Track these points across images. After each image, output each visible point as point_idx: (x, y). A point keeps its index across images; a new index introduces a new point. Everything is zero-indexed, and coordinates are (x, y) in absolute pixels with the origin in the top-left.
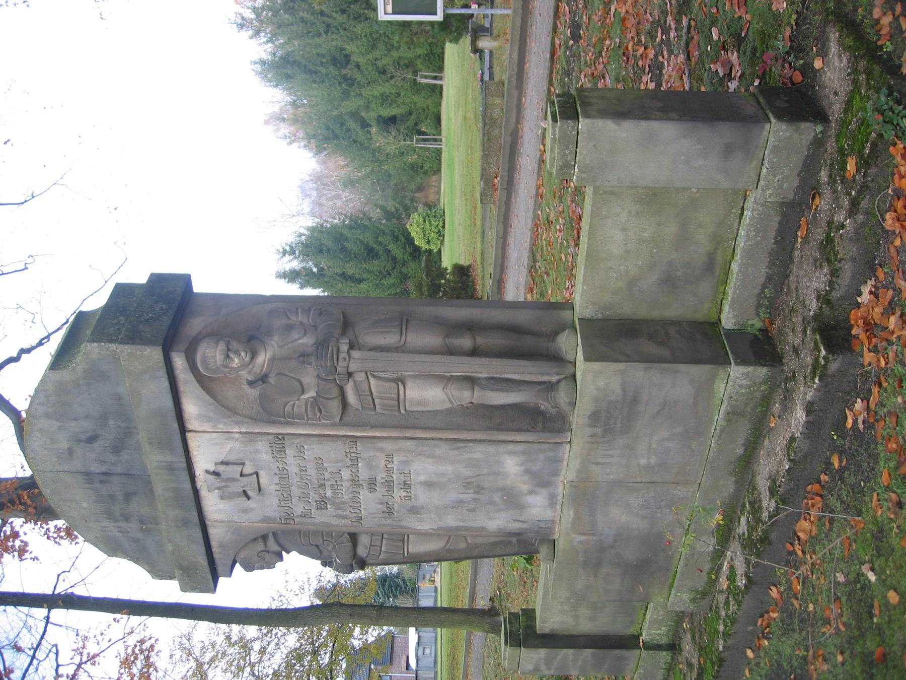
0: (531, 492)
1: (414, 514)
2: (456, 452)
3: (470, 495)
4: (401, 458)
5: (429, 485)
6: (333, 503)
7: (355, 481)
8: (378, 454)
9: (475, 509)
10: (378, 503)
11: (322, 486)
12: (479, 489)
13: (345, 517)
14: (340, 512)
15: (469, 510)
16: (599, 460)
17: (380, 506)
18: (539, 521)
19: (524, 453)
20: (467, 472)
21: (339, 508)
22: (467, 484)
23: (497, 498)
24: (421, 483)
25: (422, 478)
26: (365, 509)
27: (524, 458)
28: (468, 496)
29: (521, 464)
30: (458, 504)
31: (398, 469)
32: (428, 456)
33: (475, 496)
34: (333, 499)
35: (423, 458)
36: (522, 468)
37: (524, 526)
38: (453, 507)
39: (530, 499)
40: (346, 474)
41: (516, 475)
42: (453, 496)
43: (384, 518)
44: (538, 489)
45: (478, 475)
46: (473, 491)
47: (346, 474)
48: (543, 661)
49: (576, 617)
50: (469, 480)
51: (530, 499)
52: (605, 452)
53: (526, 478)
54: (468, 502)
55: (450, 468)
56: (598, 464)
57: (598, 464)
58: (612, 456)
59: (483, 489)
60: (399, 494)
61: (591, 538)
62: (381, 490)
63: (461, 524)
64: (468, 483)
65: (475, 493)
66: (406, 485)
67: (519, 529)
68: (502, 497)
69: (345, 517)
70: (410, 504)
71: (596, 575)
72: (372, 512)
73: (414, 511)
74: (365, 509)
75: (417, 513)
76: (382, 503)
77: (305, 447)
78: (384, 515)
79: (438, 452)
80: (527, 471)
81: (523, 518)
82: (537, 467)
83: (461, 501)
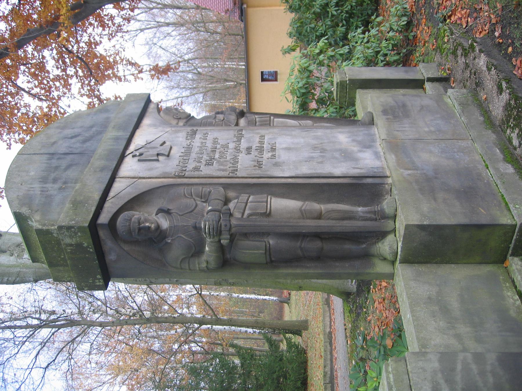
0: (360, 151)
1: (277, 166)
2: (306, 133)
3: (318, 154)
4: (270, 136)
5: (288, 149)
6: (218, 162)
7: (237, 149)
8: (255, 135)
9: (322, 161)
10: (252, 161)
11: (214, 151)
12: (323, 150)
13: (223, 170)
14: (222, 167)
15: (318, 163)
16: (398, 129)
17: (253, 163)
18: (372, 168)
19: (349, 132)
20: (314, 142)
21: (222, 165)
22: (315, 148)
23: (337, 155)
24: (283, 149)
25: (284, 146)
26: (241, 165)
27: (350, 134)
28: (316, 154)
29: (349, 137)
30: (310, 159)
31: (267, 142)
32: (288, 135)
33: (322, 154)
34: (219, 159)
35: (284, 136)
36: (350, 139)
37: (362, 171)
38: (306, 161)
39: (361, 155)
40: (232, 145)
41: (347, 142)
42: (305, 154)
43: (254, 169)
44: (365, 150)
45: (322, 143)
46: (319, 152)
47: (232, 145)
48: (440, 375)
49: (458, 337)
50: (316, 146)
51: (361, 155)
52: (399, 126)
53: (354, 144)
54: (317, 157)
55: (302, 140)
56: (398, 131)
57: (398, 131)
58: (405, 127)
59: (326, 150)
60: (267, 155)
61: (415, 172)
62: (254, 153)
63: (313, 171)
64: (315, 147)
65: (321, 152)
66: (273, 149)
67: (358, 173)
68: (341, 155)
69: (223, 170)
70: (274, 161)
71: (435, 199)
72: (246, 166)
73: (276, 165)
74: (241, 165)
75: (280, 166)
76: (254, 161)
77: (209, 133)
78: (254, 168)
79: (293, 133)
80: (354, 141)
81: (359, 166)
82: (360, 138)
83: (312, 158)
